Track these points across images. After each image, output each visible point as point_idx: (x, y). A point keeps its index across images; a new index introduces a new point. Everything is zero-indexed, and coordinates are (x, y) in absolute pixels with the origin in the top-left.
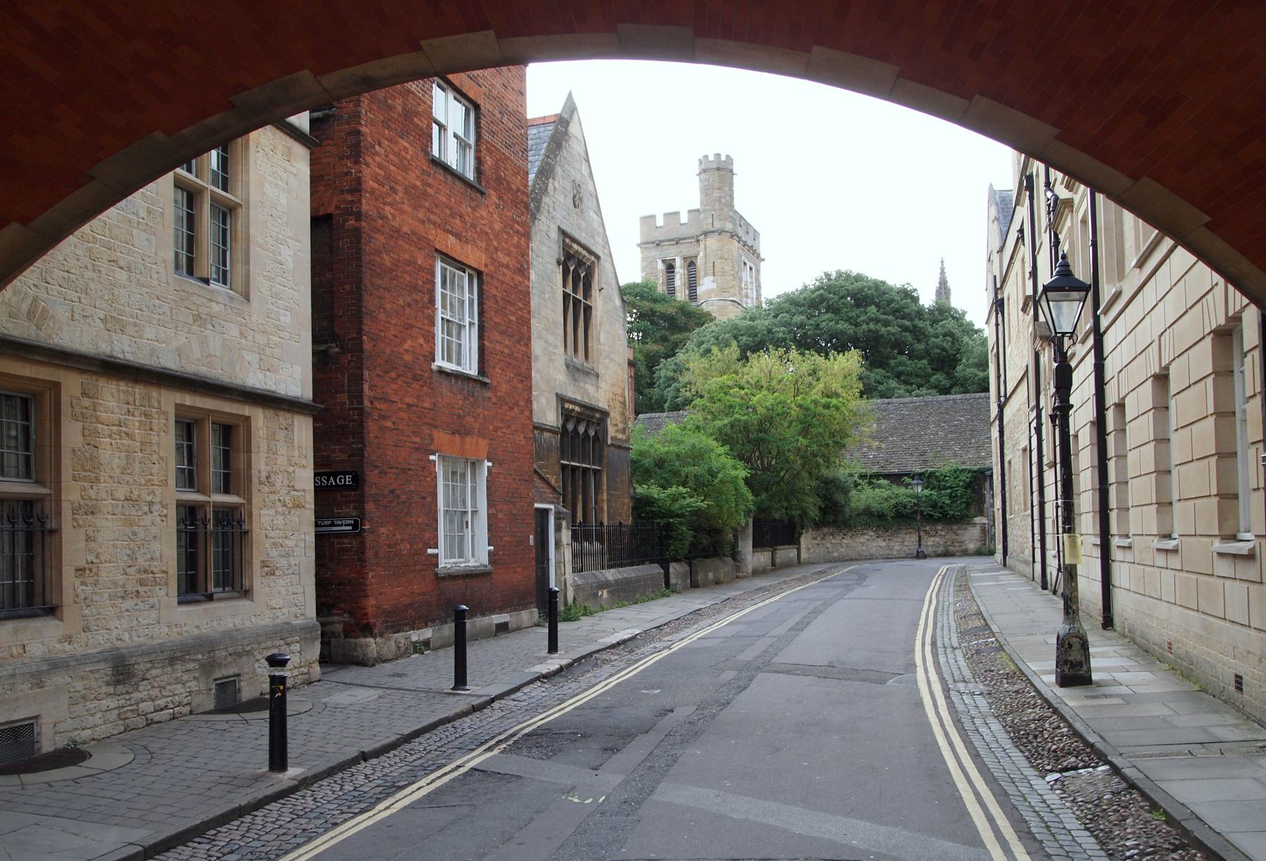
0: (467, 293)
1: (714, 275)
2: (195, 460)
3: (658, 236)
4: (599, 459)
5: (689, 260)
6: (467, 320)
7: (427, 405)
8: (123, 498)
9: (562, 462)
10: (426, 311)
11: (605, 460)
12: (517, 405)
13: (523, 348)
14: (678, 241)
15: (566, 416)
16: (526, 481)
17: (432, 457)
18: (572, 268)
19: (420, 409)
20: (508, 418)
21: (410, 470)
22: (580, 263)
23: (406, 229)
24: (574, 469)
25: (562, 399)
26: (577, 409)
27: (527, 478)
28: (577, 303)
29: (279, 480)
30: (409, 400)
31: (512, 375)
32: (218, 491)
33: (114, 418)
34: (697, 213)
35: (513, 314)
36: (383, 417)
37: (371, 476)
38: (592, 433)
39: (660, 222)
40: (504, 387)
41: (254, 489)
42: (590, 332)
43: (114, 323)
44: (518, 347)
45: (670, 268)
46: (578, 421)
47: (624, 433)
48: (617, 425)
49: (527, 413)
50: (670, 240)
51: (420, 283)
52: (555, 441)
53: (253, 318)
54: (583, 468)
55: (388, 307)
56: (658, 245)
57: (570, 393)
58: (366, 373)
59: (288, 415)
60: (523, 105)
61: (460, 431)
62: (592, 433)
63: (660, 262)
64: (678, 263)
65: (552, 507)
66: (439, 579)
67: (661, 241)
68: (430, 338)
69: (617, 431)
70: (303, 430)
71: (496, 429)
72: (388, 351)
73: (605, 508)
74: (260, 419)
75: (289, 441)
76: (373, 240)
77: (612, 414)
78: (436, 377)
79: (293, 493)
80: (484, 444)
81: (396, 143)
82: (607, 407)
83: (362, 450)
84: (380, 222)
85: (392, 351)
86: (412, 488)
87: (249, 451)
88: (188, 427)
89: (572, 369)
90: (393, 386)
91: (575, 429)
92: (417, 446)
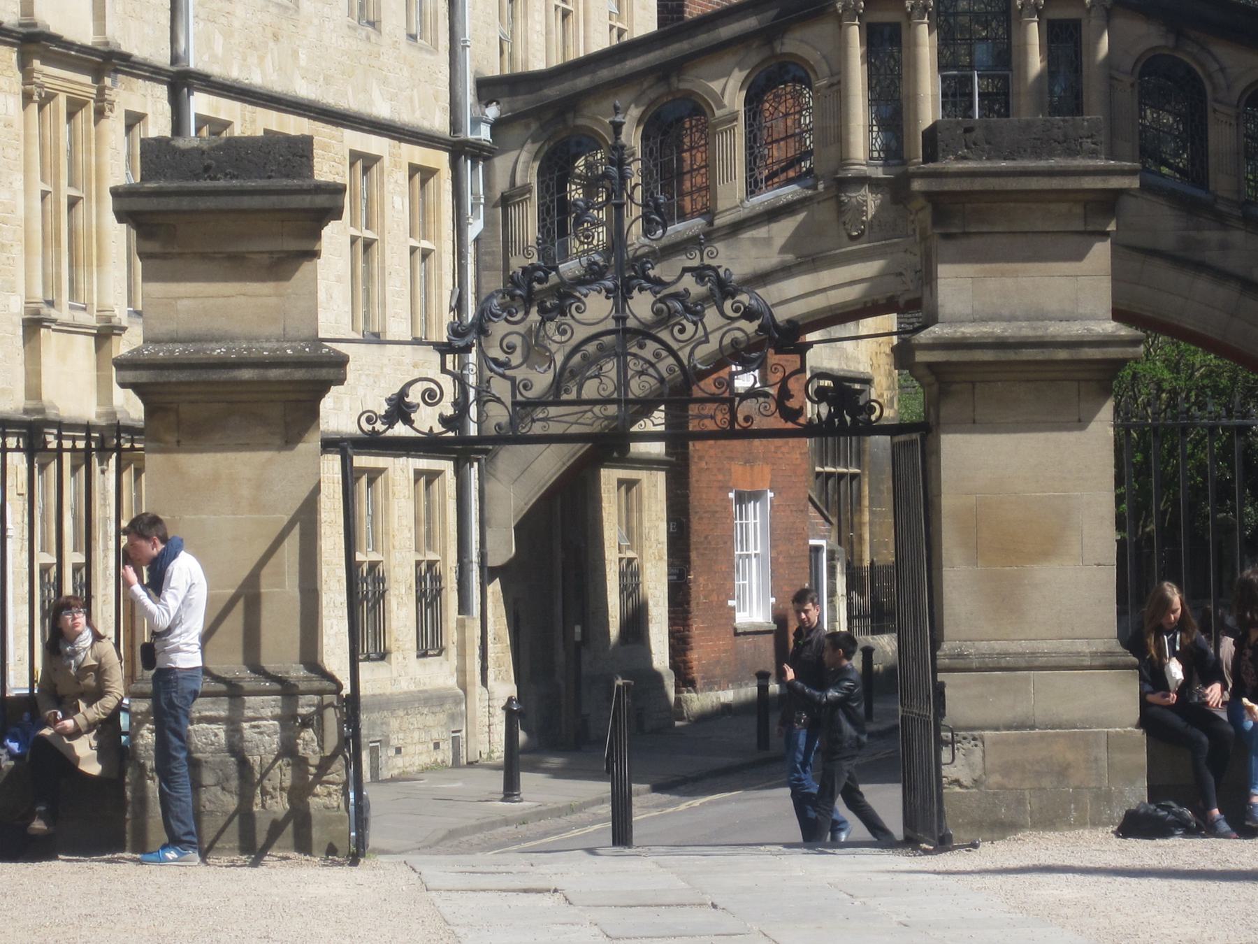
9: (818, 469)
11: (867, 458)
16: (802, 511)
24: (829, 475)
27: (802, 508)
29: (653, 535)
36: (701, 458)
65: (823, 543)
66: (736, 634)
73: (867, 536)
77: (876, 380)
79: (659, 546)
80: (767, 469)
82: (869, 370)
83: (687, 496)
92: (721, 484)
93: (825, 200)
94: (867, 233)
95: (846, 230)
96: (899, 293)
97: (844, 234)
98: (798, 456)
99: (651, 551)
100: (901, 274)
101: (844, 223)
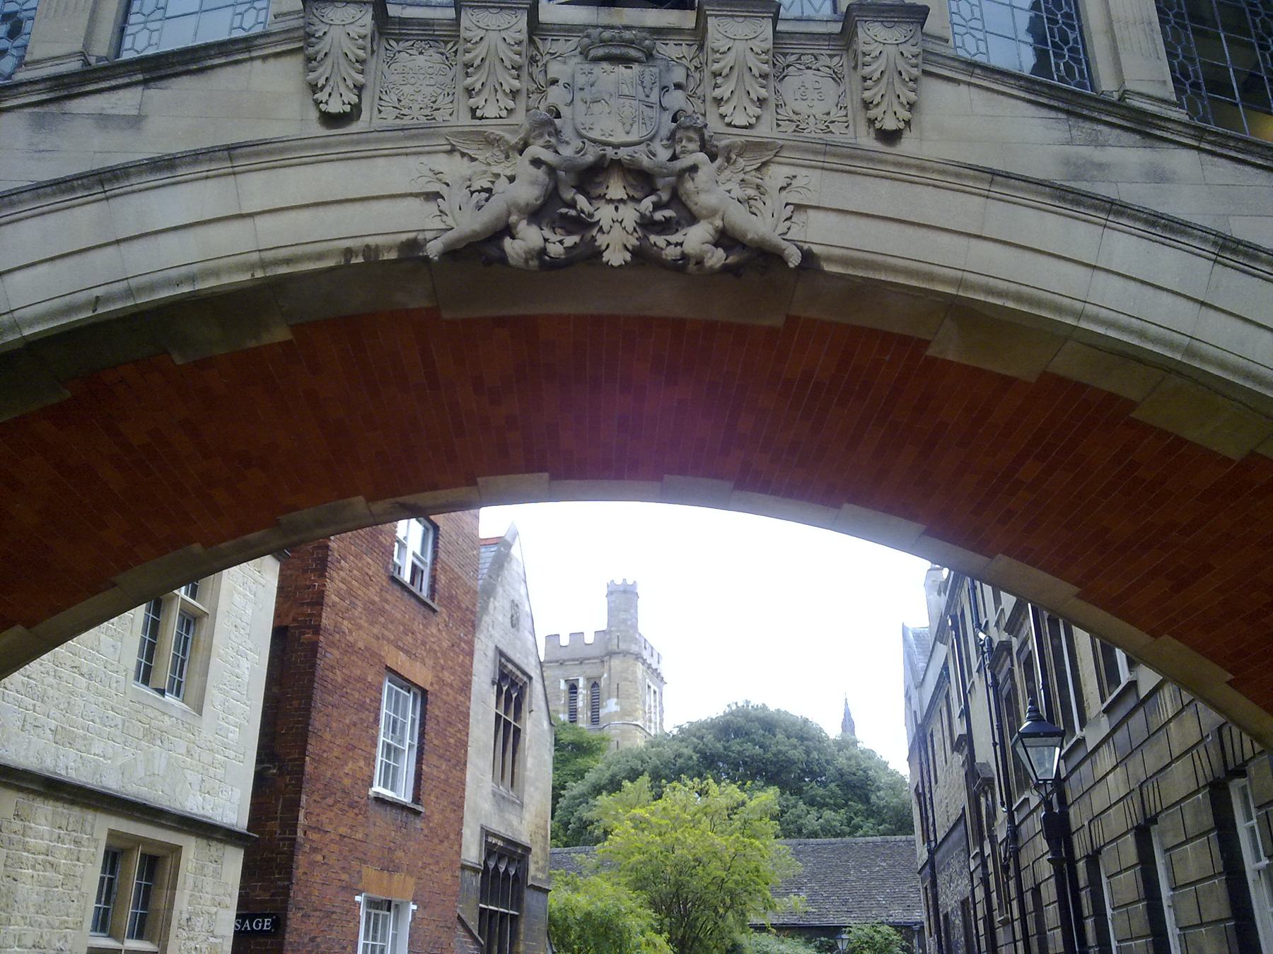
0: (411, 715)
1: (618, 697)
2: (113, 897)
3: (562, 655)
4: (518, 903)
5: (593, 681)
6: (408, 741)
7: (359, 836)
8: (30, 944)
9: (481, 905)
10: (370, 731)
12: (447, 837)
13: (459, 774)
14: (581, 661)
15: (490, 851)
16: (449, 928)
17: (358, 898)
18: (505, 689)
19: (352, 841)
20: (437, 853)
21: (333, 913)
22: (513, 684)
23: (361, 645)
25: (486, 833)
26: (500, 843)
27: (450, 925)
28: (507, 724)
29: (200, 923)
30: (342, 830)
31: (446, 804)
32: (131, 936)
33: (43, 844)
34: (602, 633)
35: (453, 736)
36: (315, 850)
37: (294, 919)
38: (512, 872)
39: (564, 641)
40: (437, 817)
41: (172, 936)
42: (517, 756)
43: (63, 737)
44: (454, 771)
45: (573, 688)
46: (500, 858)
47: (544, 872)
48: (537, 863)
49: (456, 847)
50: (574, 660)
51: (368, 701)
52: (476, 881)
53: (202, 735)
54: (501, 912)
55: (334, 725)
56: (561, 664)
57: (496, 826)
58: (304, 797)
59: (220, 846)
60: (477, 529)
61: (390, 867)
62: (512, 872)
63: (562, 682)
64: (581, 683)
67: (564, 661)
68: (370, 760)
69: (537, 869)
70: (233, 862)
71: (425, 866)
72: (329, 774)
74: (191, 848)
75: (217, 874)
76: (327, 655)
78: (372, 805)
79: (212, 940)
80: (411, 881)
81: (361, 558)
83: (288, 889)
84: (337, 636)
85: (333, 775)
86: (333, 936)
87: (174, 888)
88: (113, 858)
89: (499, 799)
90: (331, 814)
91: (496, 867)
93: (277, 55)
94: (365, 115)
95: (317, 103)
96: (429, 235)
97: (314, 115)
98: (449, 878)
99: (191, 944)
100: (437, 195)
101: (314, 88)
